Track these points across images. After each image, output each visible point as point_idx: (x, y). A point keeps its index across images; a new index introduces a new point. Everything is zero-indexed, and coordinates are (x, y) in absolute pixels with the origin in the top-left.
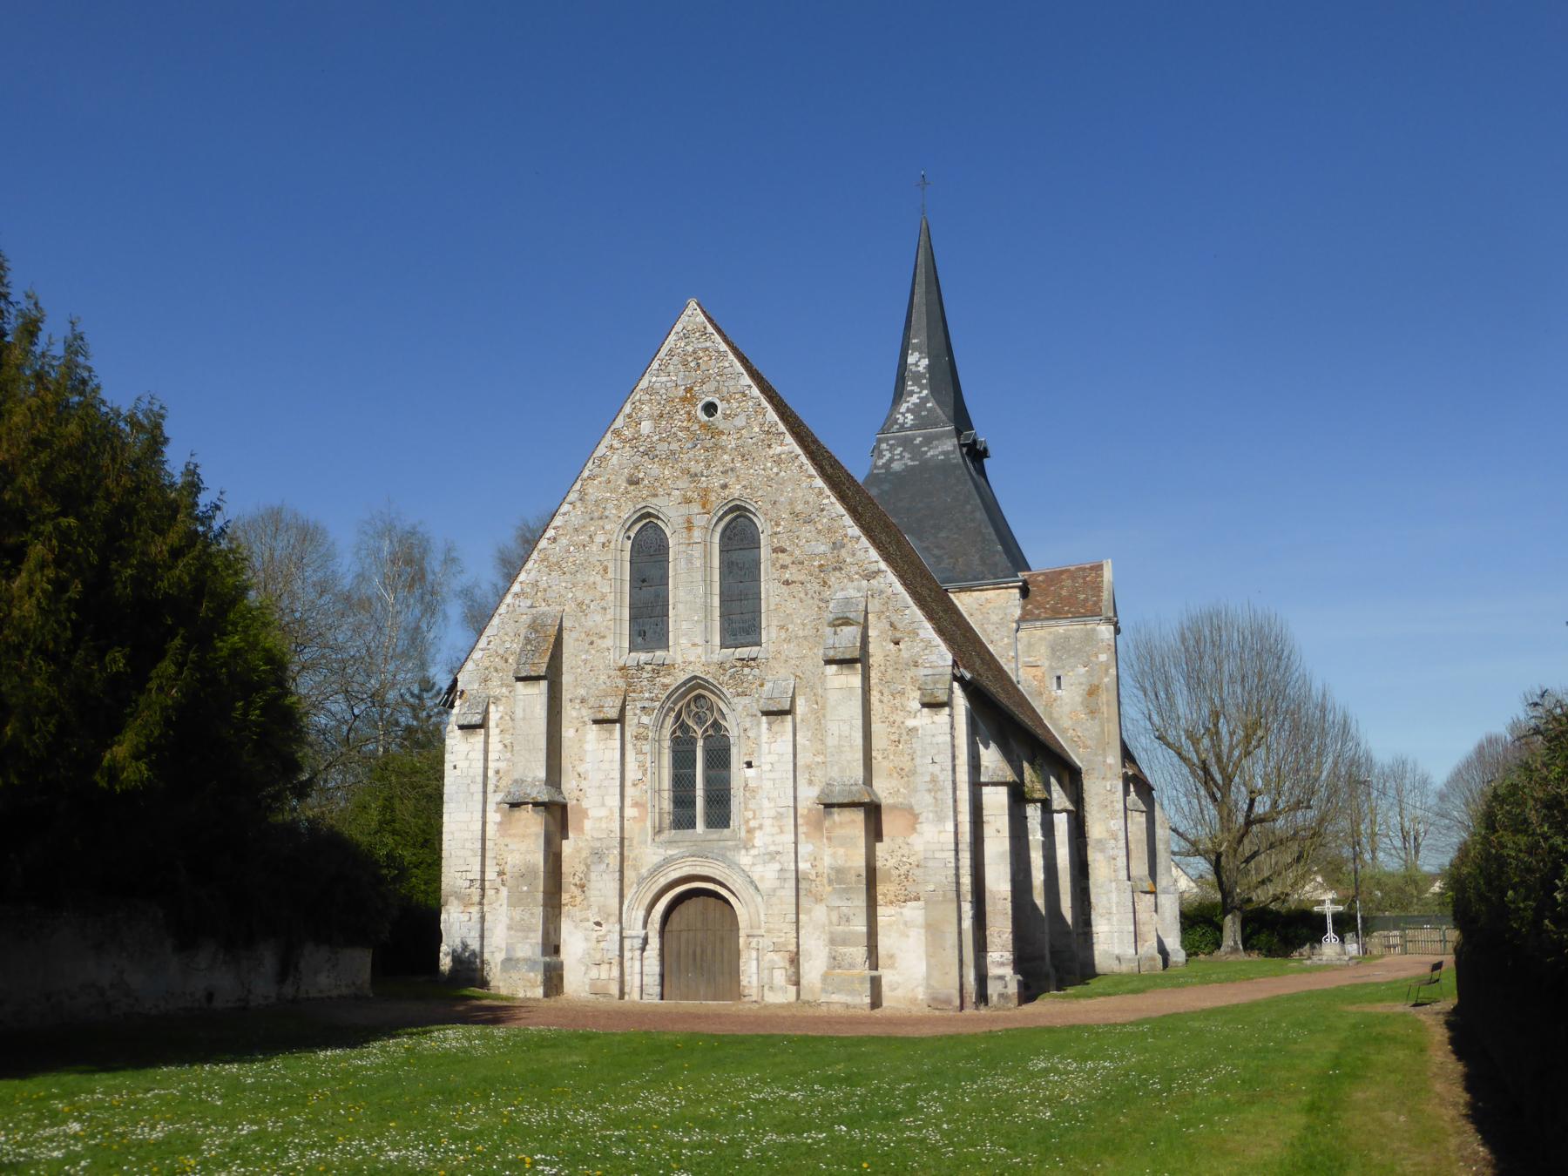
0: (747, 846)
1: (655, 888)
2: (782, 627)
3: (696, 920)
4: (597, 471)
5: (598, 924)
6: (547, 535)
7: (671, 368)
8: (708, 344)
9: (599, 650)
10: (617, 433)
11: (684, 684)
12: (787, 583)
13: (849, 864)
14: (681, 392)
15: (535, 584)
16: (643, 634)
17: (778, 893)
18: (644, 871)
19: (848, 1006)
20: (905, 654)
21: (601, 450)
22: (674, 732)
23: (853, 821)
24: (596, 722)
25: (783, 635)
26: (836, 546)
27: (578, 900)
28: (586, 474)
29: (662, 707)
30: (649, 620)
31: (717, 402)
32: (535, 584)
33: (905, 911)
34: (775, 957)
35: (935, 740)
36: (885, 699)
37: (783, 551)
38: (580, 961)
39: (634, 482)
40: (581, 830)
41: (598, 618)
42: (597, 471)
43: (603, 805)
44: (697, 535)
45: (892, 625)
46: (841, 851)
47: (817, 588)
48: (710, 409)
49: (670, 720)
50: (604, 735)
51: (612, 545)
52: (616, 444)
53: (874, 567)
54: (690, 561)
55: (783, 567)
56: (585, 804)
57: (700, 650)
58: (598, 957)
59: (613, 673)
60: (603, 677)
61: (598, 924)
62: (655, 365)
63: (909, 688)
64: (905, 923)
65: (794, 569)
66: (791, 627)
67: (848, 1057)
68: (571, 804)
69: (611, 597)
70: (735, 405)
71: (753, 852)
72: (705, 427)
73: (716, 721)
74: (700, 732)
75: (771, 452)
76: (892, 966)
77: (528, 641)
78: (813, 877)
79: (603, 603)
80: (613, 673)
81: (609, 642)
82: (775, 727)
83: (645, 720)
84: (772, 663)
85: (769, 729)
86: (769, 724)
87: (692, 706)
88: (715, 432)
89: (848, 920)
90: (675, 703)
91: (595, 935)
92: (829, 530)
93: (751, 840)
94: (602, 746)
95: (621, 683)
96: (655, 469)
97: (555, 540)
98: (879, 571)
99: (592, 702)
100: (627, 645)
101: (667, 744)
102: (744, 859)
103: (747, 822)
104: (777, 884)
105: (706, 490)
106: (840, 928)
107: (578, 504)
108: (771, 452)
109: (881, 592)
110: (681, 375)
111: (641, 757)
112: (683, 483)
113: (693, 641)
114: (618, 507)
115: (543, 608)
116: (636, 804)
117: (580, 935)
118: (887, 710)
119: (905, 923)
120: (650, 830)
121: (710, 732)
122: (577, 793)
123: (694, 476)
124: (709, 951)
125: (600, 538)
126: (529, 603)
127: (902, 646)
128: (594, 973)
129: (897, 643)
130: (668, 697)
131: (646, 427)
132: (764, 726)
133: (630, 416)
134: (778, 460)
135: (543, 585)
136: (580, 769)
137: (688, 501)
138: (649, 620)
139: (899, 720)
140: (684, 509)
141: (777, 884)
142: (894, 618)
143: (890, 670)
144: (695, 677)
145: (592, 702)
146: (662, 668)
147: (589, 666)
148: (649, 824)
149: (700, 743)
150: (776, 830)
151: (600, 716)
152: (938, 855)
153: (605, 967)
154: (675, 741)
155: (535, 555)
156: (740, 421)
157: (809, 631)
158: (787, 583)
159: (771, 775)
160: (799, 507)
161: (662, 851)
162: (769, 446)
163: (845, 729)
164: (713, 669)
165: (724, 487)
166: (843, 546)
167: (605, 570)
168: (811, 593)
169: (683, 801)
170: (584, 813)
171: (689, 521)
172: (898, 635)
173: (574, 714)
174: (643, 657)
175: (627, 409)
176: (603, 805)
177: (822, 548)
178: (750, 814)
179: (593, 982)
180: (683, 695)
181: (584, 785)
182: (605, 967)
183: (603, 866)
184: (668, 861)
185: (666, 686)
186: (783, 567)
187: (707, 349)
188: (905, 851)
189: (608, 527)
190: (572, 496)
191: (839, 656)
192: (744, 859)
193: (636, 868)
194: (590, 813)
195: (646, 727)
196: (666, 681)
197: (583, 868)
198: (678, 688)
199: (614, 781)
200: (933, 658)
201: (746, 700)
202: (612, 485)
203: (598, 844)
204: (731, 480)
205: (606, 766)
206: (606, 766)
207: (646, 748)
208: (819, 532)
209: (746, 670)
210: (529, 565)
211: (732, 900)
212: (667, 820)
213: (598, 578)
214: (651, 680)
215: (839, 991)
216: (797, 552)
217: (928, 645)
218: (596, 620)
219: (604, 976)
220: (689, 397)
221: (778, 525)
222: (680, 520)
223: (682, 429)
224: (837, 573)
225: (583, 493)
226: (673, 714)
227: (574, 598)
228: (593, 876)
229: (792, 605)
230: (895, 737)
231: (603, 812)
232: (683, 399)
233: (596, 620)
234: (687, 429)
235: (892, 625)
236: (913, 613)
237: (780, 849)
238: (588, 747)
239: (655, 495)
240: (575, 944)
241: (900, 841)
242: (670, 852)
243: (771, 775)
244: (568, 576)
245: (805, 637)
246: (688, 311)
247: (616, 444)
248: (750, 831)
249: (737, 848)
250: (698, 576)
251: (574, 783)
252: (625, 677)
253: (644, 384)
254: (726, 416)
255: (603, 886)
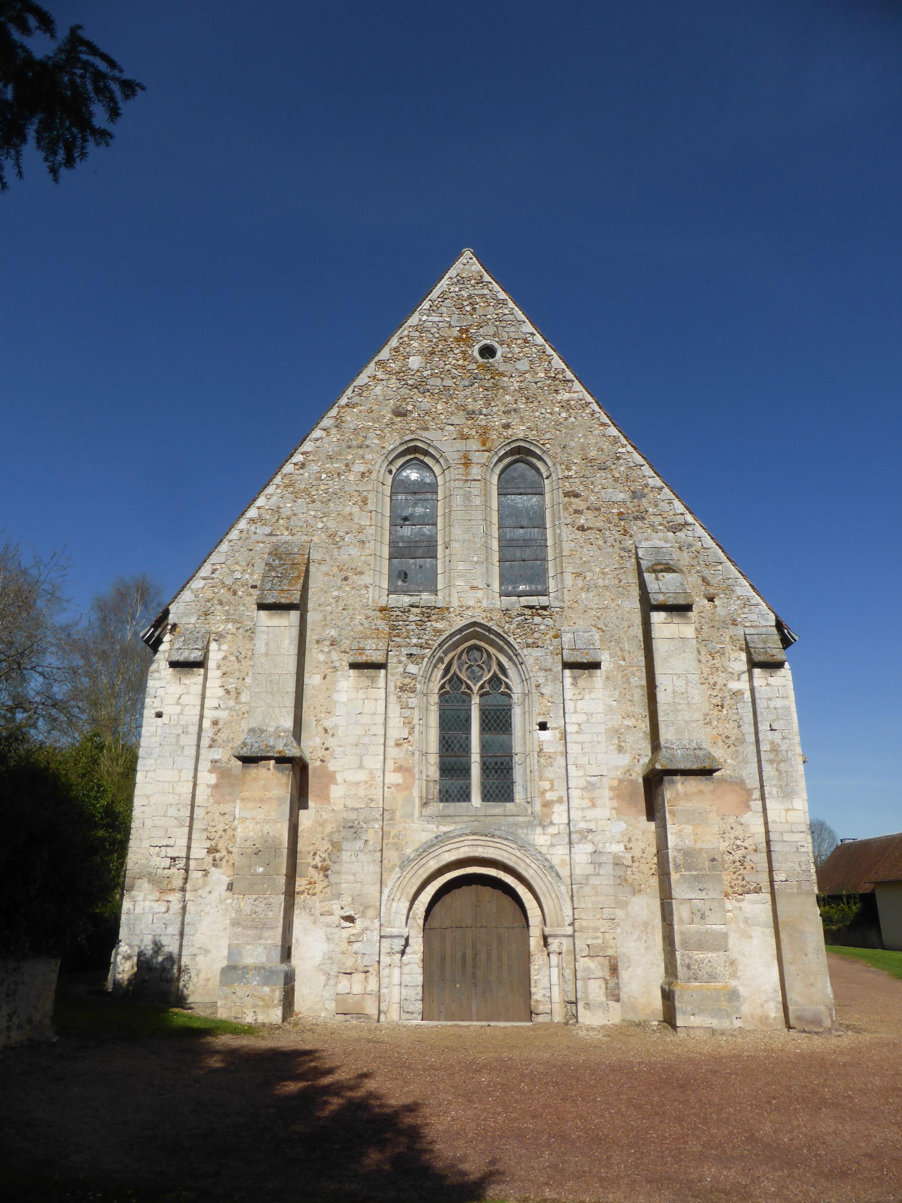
0: (543, 822)
1: (424, 874)
2: (578, 575)
3: (477, 917)
4: (356, 399)
5: (350, 919)
6: (295, 459)
7: (444, 309)
8: (486, 291)
9: (354, 584)
10: (380, 363)
11: (460, 630)
12: (582, 529)
13: (699, 845)
14: (455, 332)
15: (277, 511)
16: (404, 576)
17: (593, 881)
18: (409, 851)
19: (713, 1032)
20: (721, 612)
21: (362, 379)
22: (443, 687)
23: (701, 792)
24: (354, 666)
25: (580, 583)
26: (636, 495)
27: (318, 888)
28: (343, 401)
29: (433, 656)
30: (413, 559)
31: (496, 345)
32: (277, 511)
33: (744, 905)
34: (592, 964)
35: (772, 704)
36: (703, 659)
37: (577, 496)
38: (319, 968)
39: (400, 413)
40: (325, 798)
41: (355, 551)
42: (356, 399)
43: (361, 767)
44: (476, 471)
45: (704, 579)
46: (688, 829)
47: (617, 536)
48: (488, 352)
49: (439, 673)
50: (366, 682)
51: (374, 476)
52: (380, 375)
53: (680, 520)
54: (467, 497)
55: (576, 512)
56: (332, 766)
57: (480, 594)
58: (349, 963)
59: (371, 613)
60: (359, 618)
61: (350, 919)
62: (426, 304)
63: (729, 647)
64: (746, 920)
65: (590, 515)
66: (589, 575)
67: (671, 1105)
68: (313, 765)
69: (371, 531)
70: (517, 350)
71: (552, 830)
72: (487, 368)
73: (495, 675)
74: (475, 688)
75: (559, 397)
76: (536, 987)
77: (270, 567)
78: (628, 862)
79: (361, 537)
80: (371, 613)
81: (367, 579)
82: (581, 683)
83: (412, 668)
84: (567, 612)
85: (575, 684)
86: (574, 678)
87: (464, 657)
88: (497, 374)
89: (703, 917)
90: (446, 653)
91: (345, 934)
92: (627, 479)
93: (549, 815)
94: (361, 694)
95: (383, 625)
96: (426, 402)
97: (303, 466)
98: (686, 524)
99: (346, 644)
100: (385, 585)
101: (435, 698)
102: (540, 839)
103: (544, 792)
104: (590, 869)
105: (485, 427)
106: (694, 927)
107: (334, 431)
108: (559, 397)
109: (690, 546)
110: (455, 317)
111: (407, 713)
112: (459, 418)
113: (469, 586)
114: (381, 437)
115: (286, 537)
116: (399, 769)
117: (320, 933)
118: (706, 671)
119: (746, 920)
120: (417, 800)
121: (487, 688)
122: (321, 753)
123: (471, 414)
124: (483, 956)
125: (359, 467)
126: (268, 530)
127: (717, 602)
128: (344, 985)
129: (711, 600)
130: (440, 645)
131: (415, 362)
132: (568, 681)
133: (396, 350)
134: (566, 406)
135: (286, 511)
136: (328, 723)
137: (465, 437)
138: (413, 559)
139: (720, 682)
140: (460, 445)
141: (590, 869)
142: (706, 573)
143: (705, 627)
144: (475, 624)
145: (346, 644)
146: (442, 611)
147: (341, 604)
148: (416, 793)
149: (476, 700)
150: (586, 803)
151: (362, 659)
152: (786, 837)
153: (358, 977)
154: (443, 696)
155: (278, 479)
156: (523, 365)
157: (610, 581)
158: (582, 529)
159: (580, 738)
160: (593, 453)
161: (432, 827)
162: (556, 391)
163: (680, 684)
164: (497, 615)
165: (507, 426)
166: (644, 496)
167: (365, 501)
168: (611, 540)
169: (453, 767)
170: (331, 778)
171: (466, 457)
172: (712, 591)
173: (322, 657)
174: (406, 600)
175: (394, 342)
176: (361, 767)
177: (621, 496)
178: (546, 785)
179: (340, 998)
180: (455, 646)
181: (331, 742)
182: (358, 977)
183: (360, 844)
184: (440, 840)
185: (438, 632)
186: (576, 512)
187: (484, 296)
188: (738, 831)
189: (369, 457)
190: (326, 422)
191: (671, 601)
192: (540, 839)
193: (398, 847)
194: (339, 778)
195: (413, 677)
196: (439, 625)
197: (327, 845)
198: (452, 635)
199: (373, 738)
200: (753, 617)
201: (537, 652)
202: (374, 415)
203: (353, 816)
204: (514, 420)
205: (365, 719)
206: (365, 719)
207: (413, 701)
208: (616, 480)
209: (537, 619)
210: (271, 489)
211: (521, 890)
212: (435, 789)
213: (356, 509)
214: (420, 624)
215: (701, 1012)
216: (593, 498)
217: (746, 603)
218: (351, 553)
219: (357, 989)
220: (465, 337)
221: (569, 469)
222: (456, 455)
223: (456, 367)
224: (639, 523)
225: (339, 423)
226: (442, 667)
227: (325, 529)
228: (345, 856)
229: (588, 553)
230: (717, 701)
231: (361, 776)
232: (458, 340)
233: (351, 553)
234: (463, 367)
235: (704, 579)
236: (727, 570)
237: (592, 826)
238: (342, 697)
239: (426, 429)
240: (312, 945)
241: (731, 820)
242: (444, 829)
243: (580, 738)
244: (318, 505)
245: (606, 587)
246: (463, 260)
247: (380, 375)
248: (547, 805)
249: (530, 825)
250: (478, 515)
251: (318, 740)
252: (387, 619)
253: (414, 320)
254: (507, 360)
255: (357, 869)
